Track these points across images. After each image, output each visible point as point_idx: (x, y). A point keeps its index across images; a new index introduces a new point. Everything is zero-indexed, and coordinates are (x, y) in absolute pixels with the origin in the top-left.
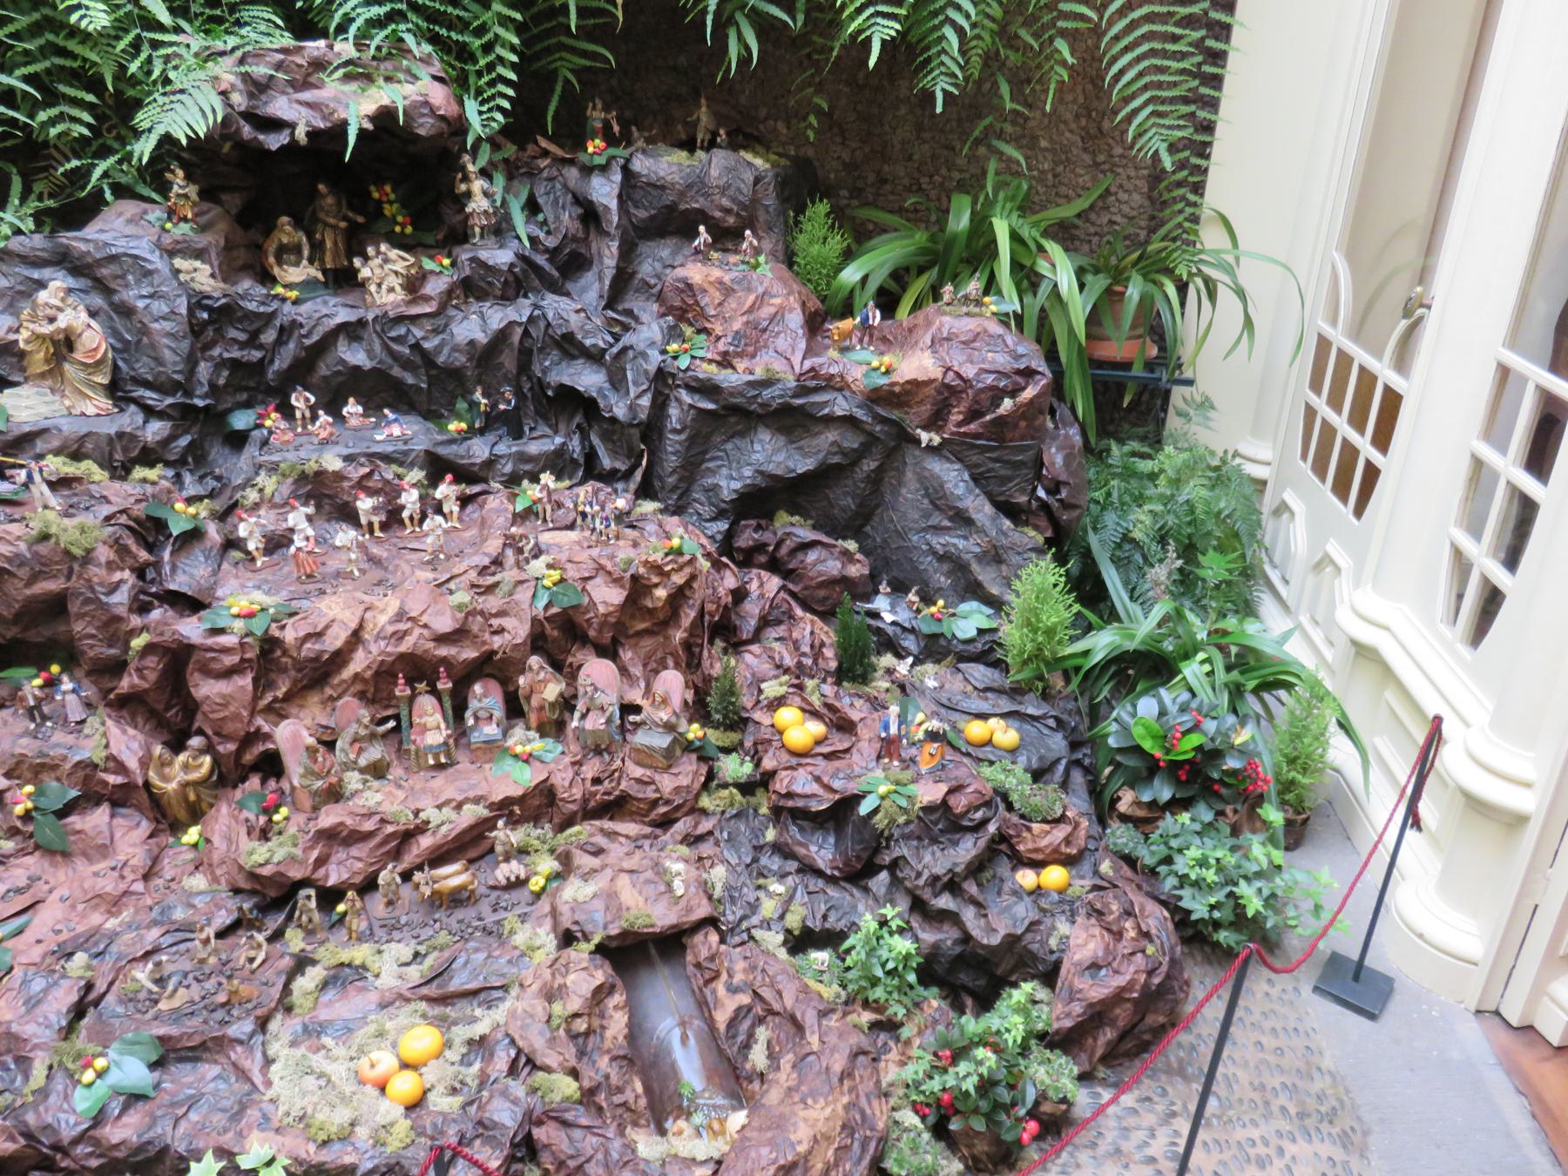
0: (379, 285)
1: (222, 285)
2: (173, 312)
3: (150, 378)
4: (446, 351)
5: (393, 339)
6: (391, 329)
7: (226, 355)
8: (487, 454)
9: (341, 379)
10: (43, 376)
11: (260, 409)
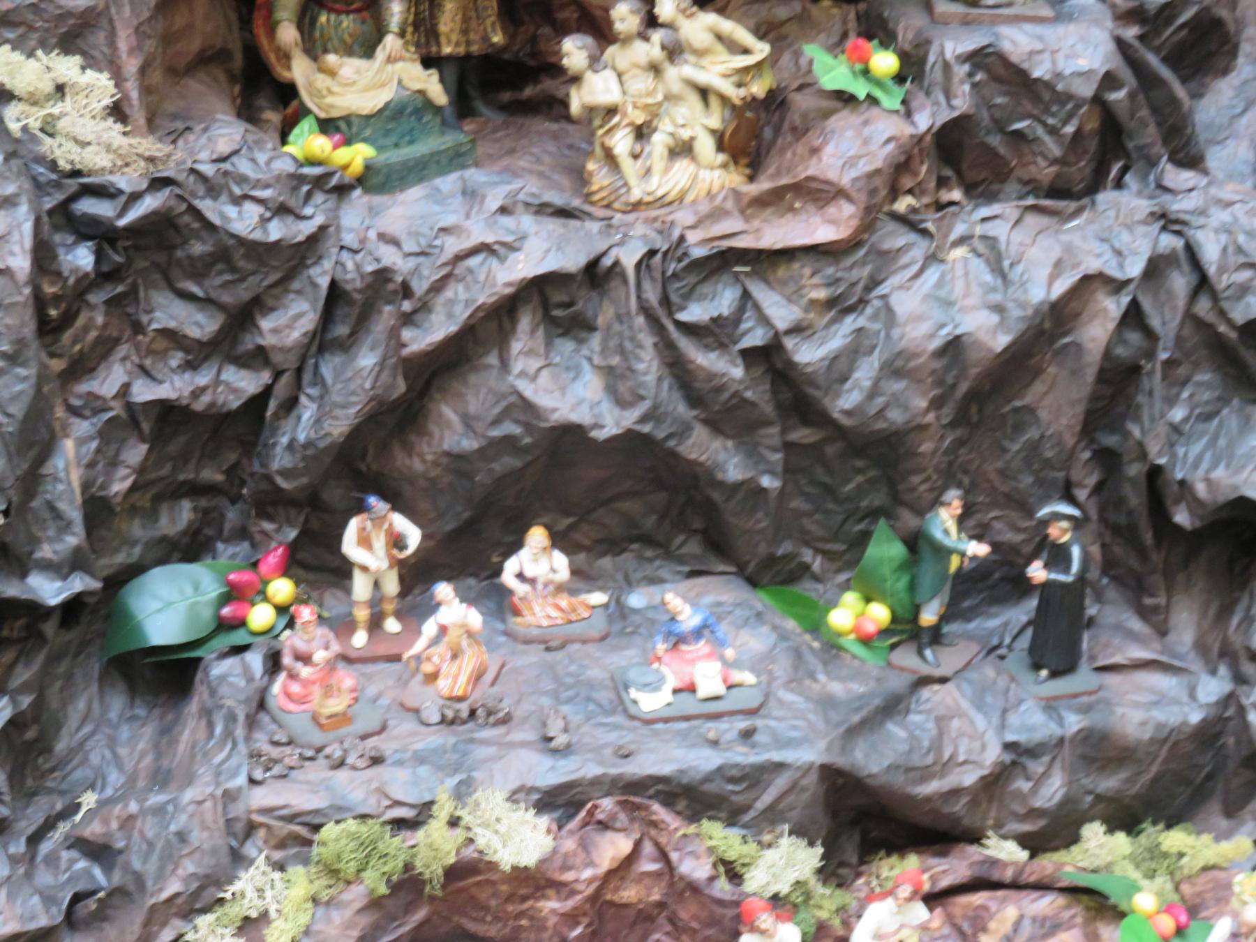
0: (642, 133)
1: (149, 145)
4: (865, 372)
5: (690, 329)
6: (688, 296)
7: (144, 392)
8: (993, 755)
11: (229, 554)
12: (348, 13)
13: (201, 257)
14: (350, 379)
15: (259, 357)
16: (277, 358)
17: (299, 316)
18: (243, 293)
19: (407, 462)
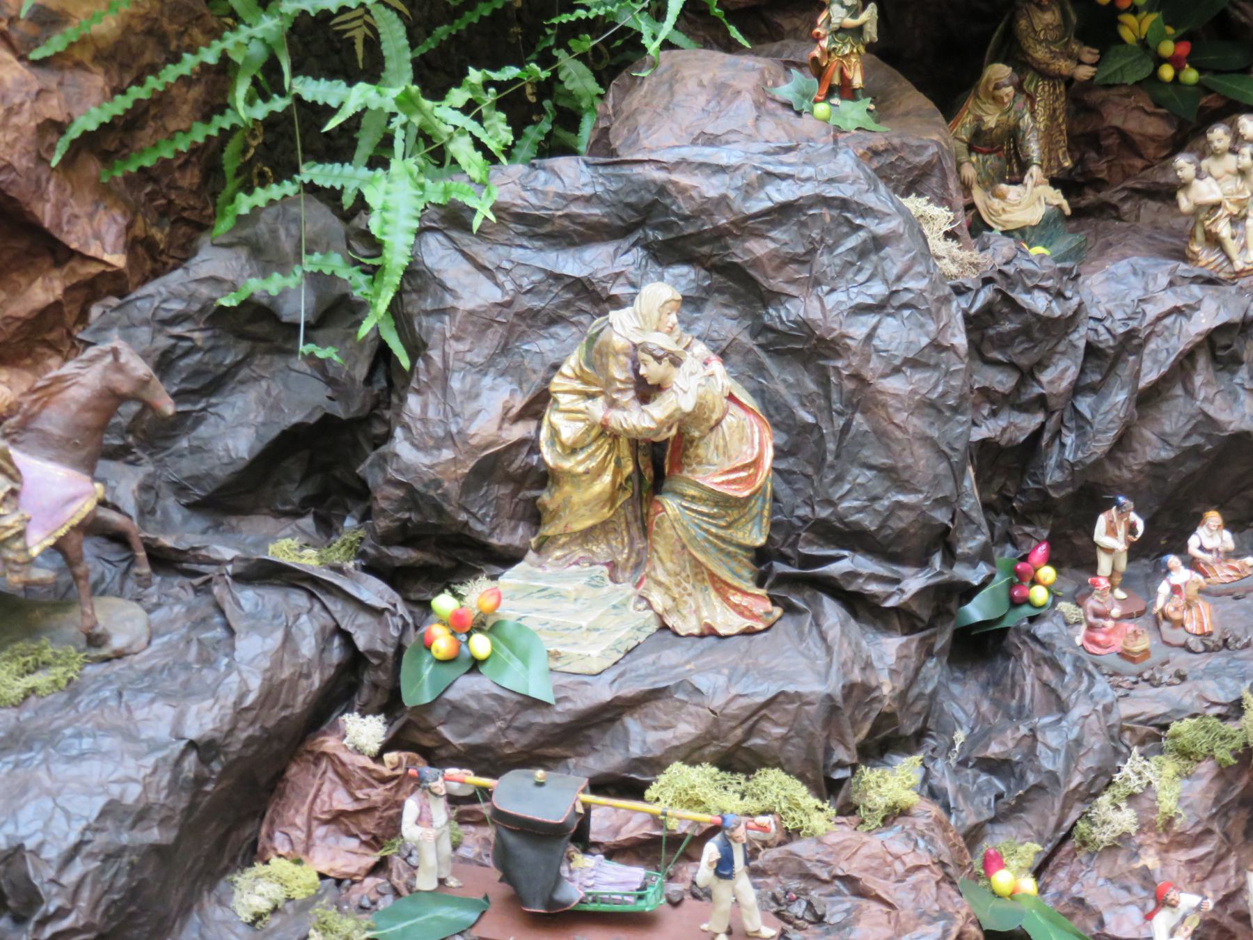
2: (936, 346)
3: (869, 522)
7: (978, 434)
9: (1192, 465)
10: (587, 535)
12: (989, 153)
13: (1009, 333)
14: (1107, 413)
15: (1041, 402)
16: (1052, 402)
17: (1066, 369)
18: (1035, 355)
19: (1117, 472)
